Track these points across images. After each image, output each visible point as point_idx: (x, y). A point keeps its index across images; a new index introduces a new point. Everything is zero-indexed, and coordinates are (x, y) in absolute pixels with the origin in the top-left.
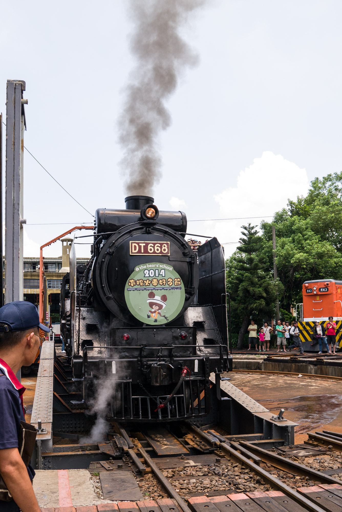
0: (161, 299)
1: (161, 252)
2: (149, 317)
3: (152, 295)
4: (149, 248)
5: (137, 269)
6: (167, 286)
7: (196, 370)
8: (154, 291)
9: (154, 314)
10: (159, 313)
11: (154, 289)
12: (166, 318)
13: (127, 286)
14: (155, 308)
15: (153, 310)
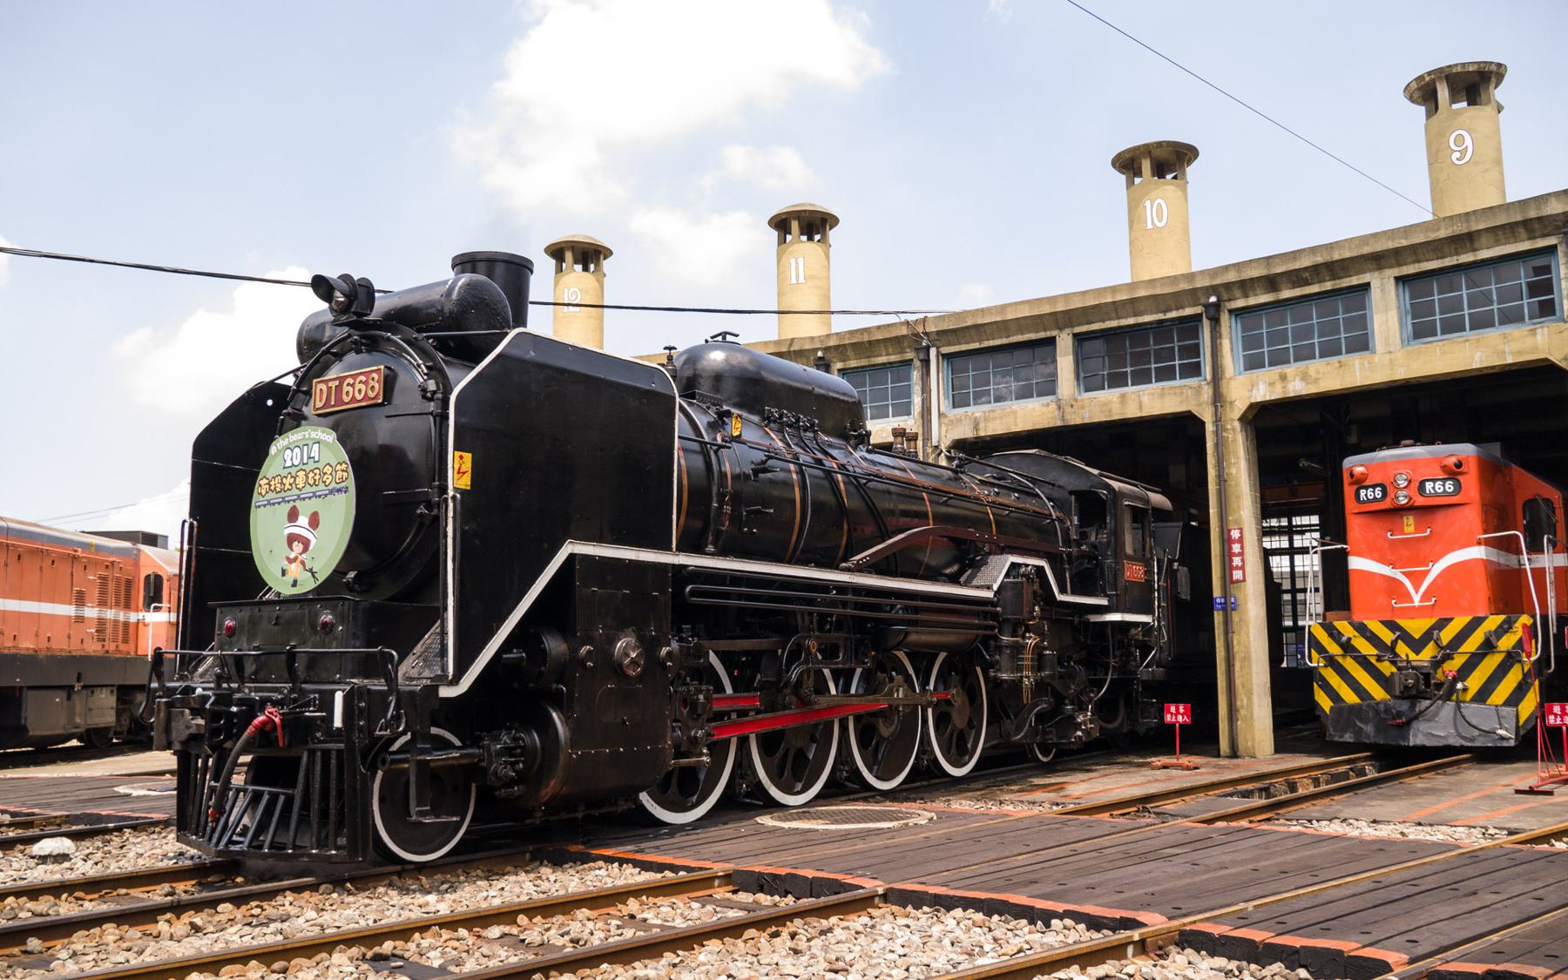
0: (311, 524)
1: (366, 397)
2: (284, 573)
3: (293, 516)
4: (346, 388)
5: (273, 450)
6: (322, 486)
7: (338, 722)
8: (298, 504)
9: (293, 566)
10: (303, 563)
11: (299, 498)
12: (313, 574)
13: (256, 498)
14: (298, 547)
15: (292, 556)
